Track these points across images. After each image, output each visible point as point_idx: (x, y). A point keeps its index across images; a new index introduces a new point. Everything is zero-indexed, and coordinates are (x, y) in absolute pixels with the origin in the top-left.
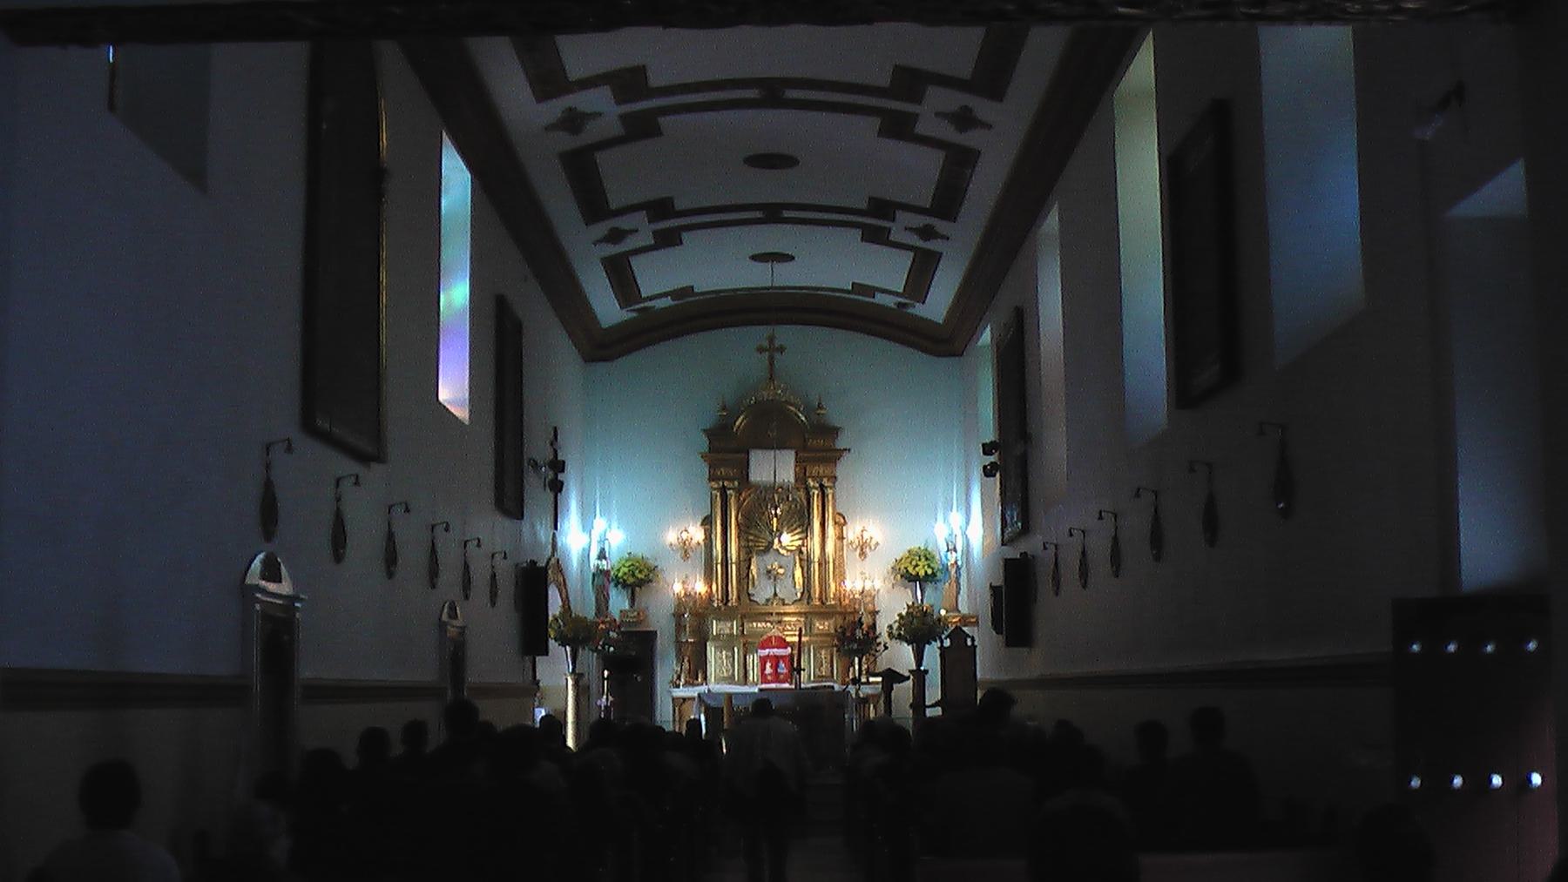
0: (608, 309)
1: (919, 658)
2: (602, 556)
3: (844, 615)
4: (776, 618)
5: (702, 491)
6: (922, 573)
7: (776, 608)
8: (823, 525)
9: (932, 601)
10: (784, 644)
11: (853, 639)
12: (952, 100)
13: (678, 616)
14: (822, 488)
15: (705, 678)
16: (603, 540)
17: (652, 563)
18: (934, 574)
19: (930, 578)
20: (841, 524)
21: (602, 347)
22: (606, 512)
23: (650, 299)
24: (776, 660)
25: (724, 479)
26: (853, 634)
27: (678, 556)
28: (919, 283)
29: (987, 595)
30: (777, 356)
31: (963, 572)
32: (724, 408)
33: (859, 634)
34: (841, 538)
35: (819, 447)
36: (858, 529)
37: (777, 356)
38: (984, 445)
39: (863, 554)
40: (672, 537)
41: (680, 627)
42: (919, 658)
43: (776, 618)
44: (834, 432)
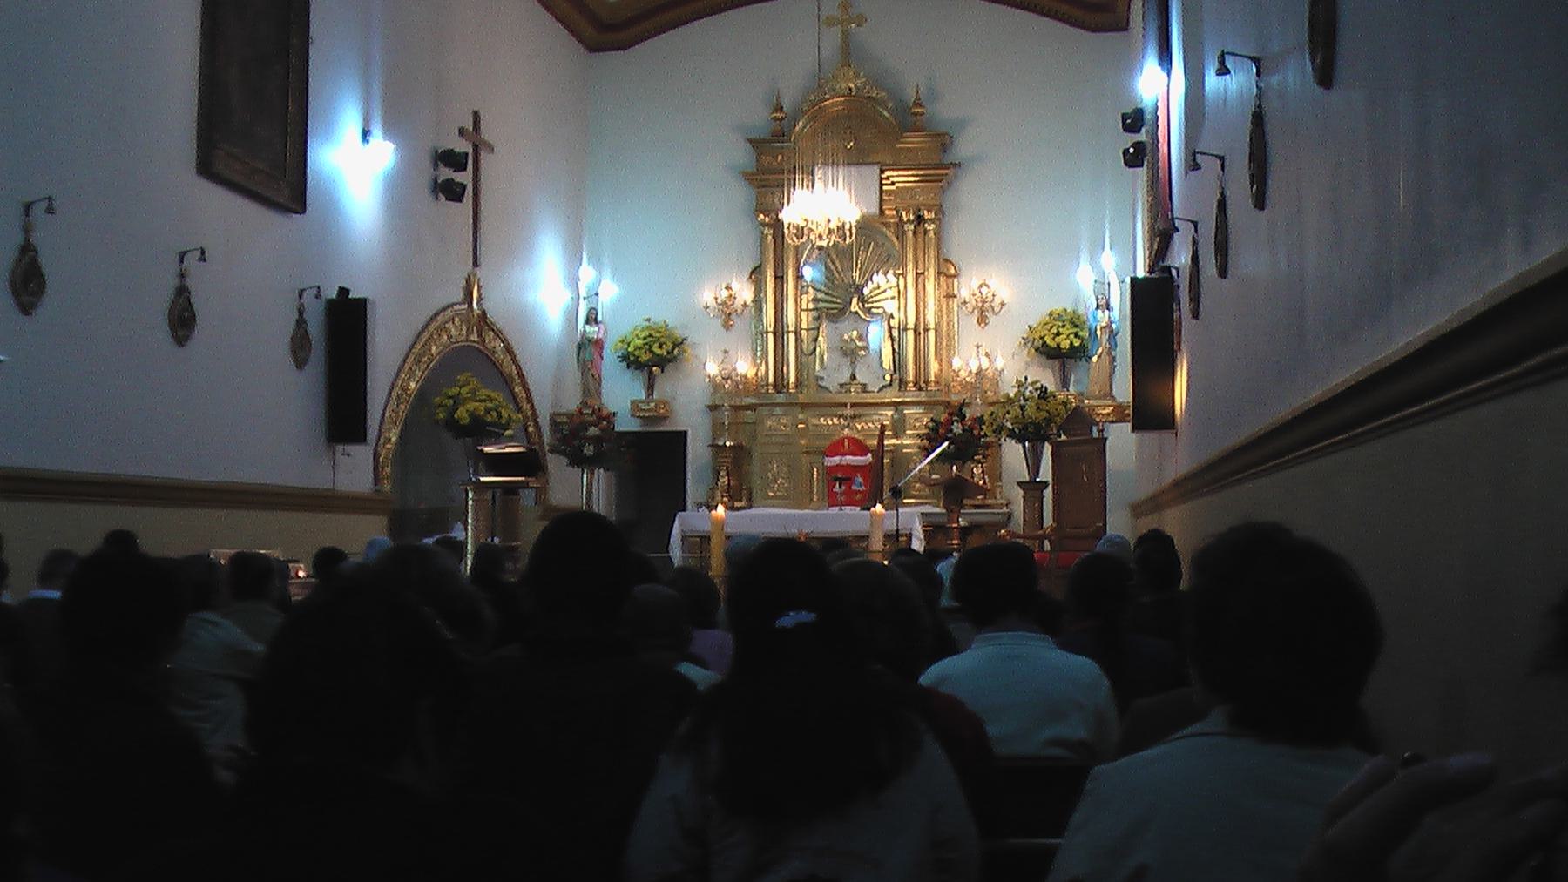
1: (1034, 465)
2: (592, 319)
3: (948, 404)
4: (849, 411)
6: (1065, 345)
7: (854, 396)
9: (1080, 388)
10: (861, 449)
14: (920, 220)
15: (750, 500)
17: (679, 333)
19: (1079, 353)
22: (596, 262)
33: (957, 428)
36: (975, 284)
38: (1124, 117)
39: (983, 320)
40: (708, 296)
41: (717, 429)
42: (1034, 465)
43: (849, 411)
44: (943, 141)
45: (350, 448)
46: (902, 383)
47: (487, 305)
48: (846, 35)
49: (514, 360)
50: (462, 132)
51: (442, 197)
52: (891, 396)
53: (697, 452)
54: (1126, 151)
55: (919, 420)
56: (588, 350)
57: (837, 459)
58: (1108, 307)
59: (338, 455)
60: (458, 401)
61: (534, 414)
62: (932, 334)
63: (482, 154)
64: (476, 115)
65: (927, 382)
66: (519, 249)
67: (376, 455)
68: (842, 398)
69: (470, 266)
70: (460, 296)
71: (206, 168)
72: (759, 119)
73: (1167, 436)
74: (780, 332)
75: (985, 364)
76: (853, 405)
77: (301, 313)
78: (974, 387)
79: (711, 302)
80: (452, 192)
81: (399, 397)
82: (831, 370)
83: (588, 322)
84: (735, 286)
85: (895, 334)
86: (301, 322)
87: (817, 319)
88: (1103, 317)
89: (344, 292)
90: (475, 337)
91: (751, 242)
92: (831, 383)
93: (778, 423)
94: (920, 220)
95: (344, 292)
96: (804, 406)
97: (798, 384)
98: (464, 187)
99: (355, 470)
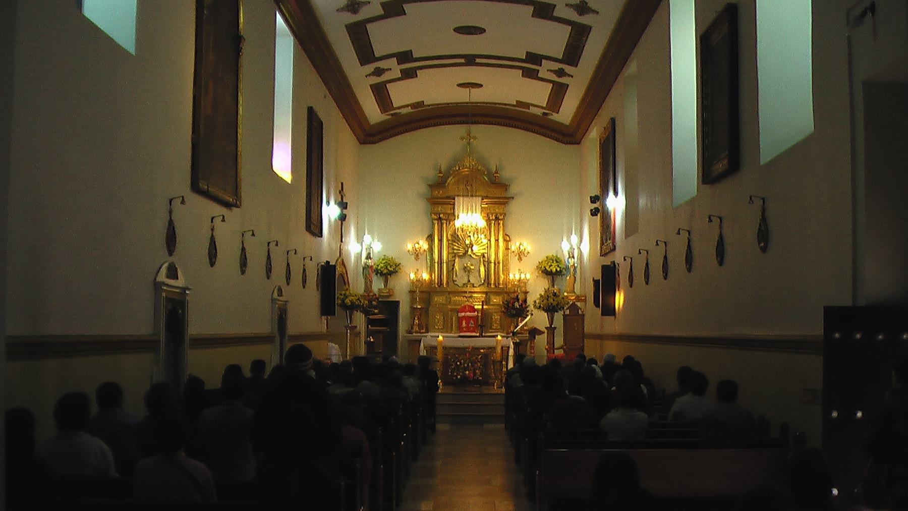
0: (373, 113)
2: (368, 257)
3: (508, 293)
6: (554, 270)
7: (469, 289)
11: (513, 307)
12: (556, 66)
13: (412, 292)
17: (397, 261)
18: (561, 271)
19: (559, 273)
21: (371, 136)
23: (399, 108)
24: (468, 319)
26: (513, 305)
31: (578, 270)
33: (517, 305)
34: (507, 249)
36: (518, 244)
38: (591, 198)
39: (520, 259)
40: (410, 247)
41: (413, 301)
44: (505, 187)
46: (489, 284)
53: (404, 309)
55: (496, 300)
57: (463, 314)
58: (573, 257)
60: (346, 296)
68: (464, 289)
72: (431, 174)
73: (612, 318)
75: (523, 277)
78: (518, 286)
84: (421, 242)
88: (571, 261)
91: (426, 222)
93: (439, 299)
94: (497, 219)
96: (450, 293)
97: (448, 283)
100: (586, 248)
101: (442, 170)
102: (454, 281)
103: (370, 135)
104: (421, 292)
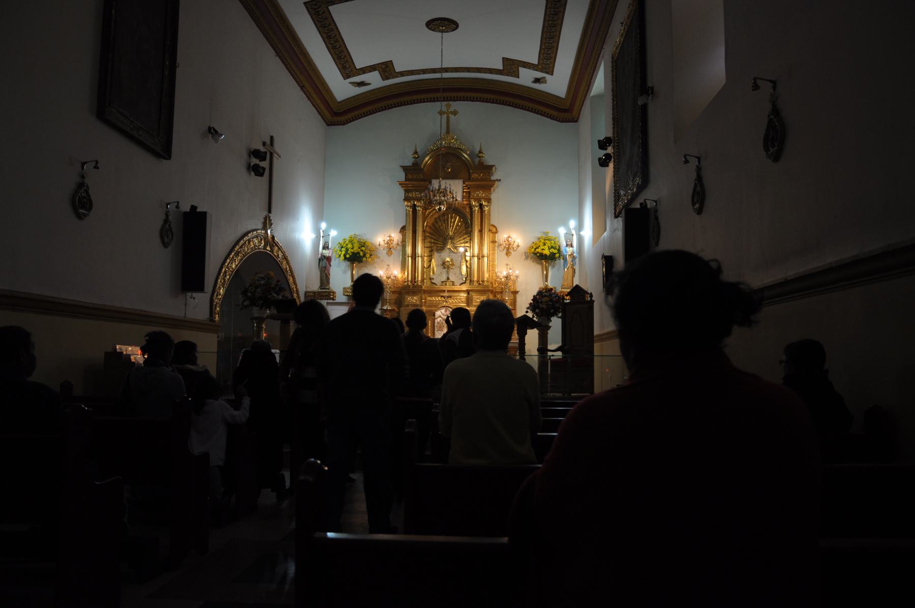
0: (342, 88)
2: (326, 247)
5: (403, 208)
7: (449, 287)
8: (481, 231)
14: (481, 206)
16: (326, 235)
20: (494, 231)
21: (337, 114)
23: (364, 70)
25: (415, 199)
27: (385, 252)
28: (547, 62)
29: (600, 262)
30: (452, 116)
31: (577, 260)
32: (416, 153)
34: (494, 242)
35: (480, 176)
36: (506, 236)
37: (452, 116)
38: (599, 141)
39: (508, 254)
43: (446, 294)
45: (195, 295)
47: (275, 235)
48: (448, 118)
49: (288, 263)
50: (264, 144)
51: (253, 173)
52: (464, 288)
54: (600, 159)
56: (324, 263)
58: (572, 246)
59: (188, 297)
61: (297, 291)
62: (486, 259)
63: (275, 160)
64: (272, 138)
65: (483, 281)
66: (290, 212)
67: (212, 300)
68: (443, 288)
69: (265, 213)
70: (260, 226)
71: (101, 115)
74: (414, 256)
76: (448, 291)
77: (167, 215)
79: (382, 243)
80: (258, 171)
81: (225, 272)
82: (439, 276)
83: (324, 248)
85: (468, 258)
86: (166, 221)
87: (431, 251)
88: (569, 250)
89: (194, 208)
90: (268, 248)
92: (437, 281)
95: (194, 208)
96: (425, 292)
97: (423, 280)
98: (264, 169)
99: (197, 306)
100: (588, 233)
101: (418, 150)
102: (431, 279)
103: (336, 114)
104: (393, 292)
